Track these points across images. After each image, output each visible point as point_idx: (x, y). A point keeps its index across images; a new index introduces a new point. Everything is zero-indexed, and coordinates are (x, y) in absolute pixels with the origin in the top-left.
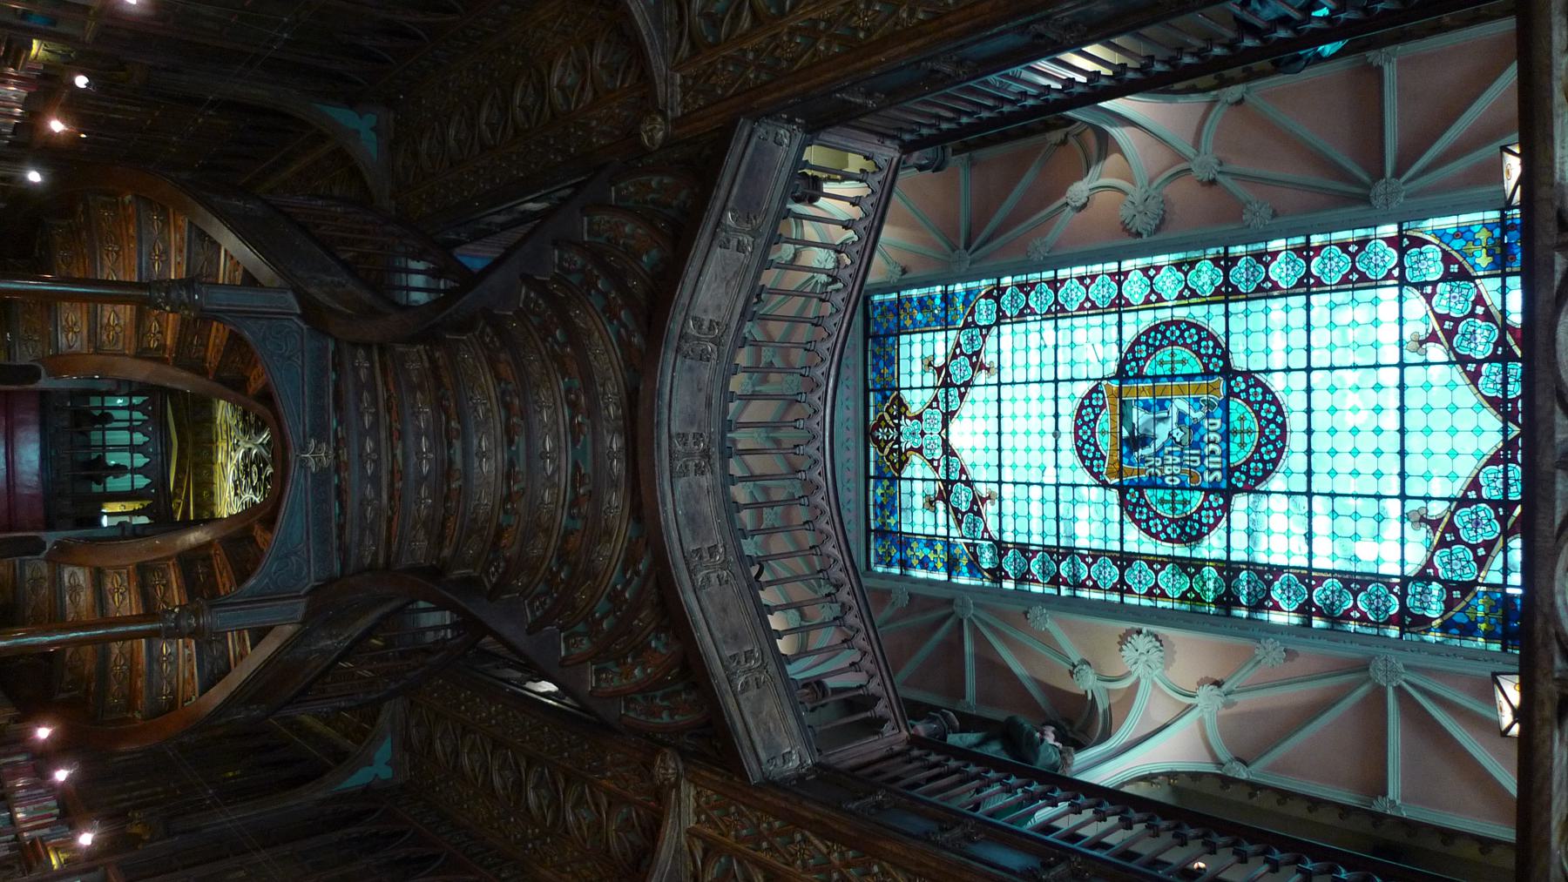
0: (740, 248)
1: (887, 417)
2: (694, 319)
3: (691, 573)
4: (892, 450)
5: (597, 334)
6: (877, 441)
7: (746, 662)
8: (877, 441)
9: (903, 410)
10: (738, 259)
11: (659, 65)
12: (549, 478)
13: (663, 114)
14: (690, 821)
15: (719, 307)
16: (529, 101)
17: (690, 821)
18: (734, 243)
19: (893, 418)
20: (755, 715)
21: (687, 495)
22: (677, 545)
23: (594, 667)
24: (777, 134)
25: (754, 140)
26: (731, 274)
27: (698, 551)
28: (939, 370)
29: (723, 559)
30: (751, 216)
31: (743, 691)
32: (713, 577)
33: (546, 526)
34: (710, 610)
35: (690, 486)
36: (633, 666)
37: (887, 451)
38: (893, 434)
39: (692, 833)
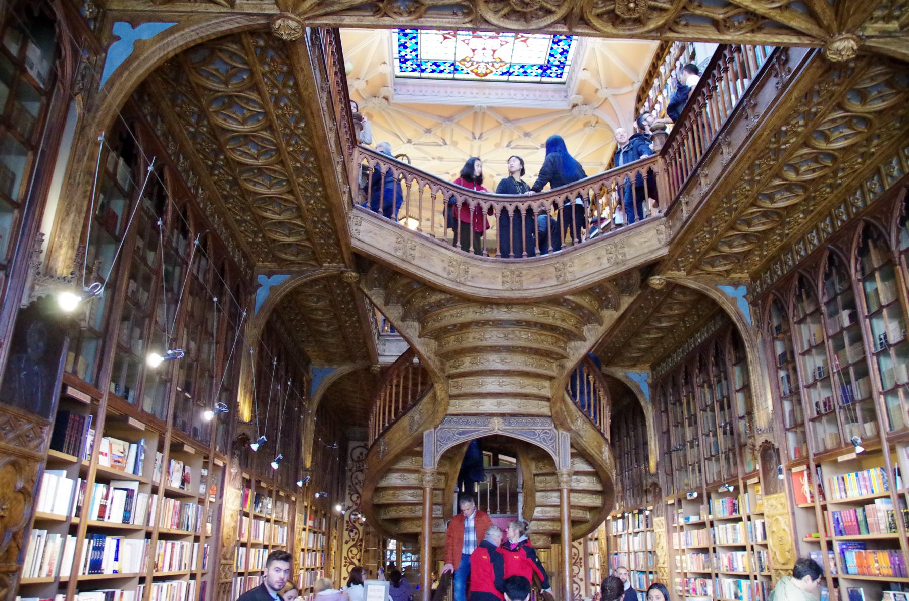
1: (472, 68)
4: (493, 66)
6: (486, 74)
8: (486, 74)
9: (468, 59)
11: (320, 273)
13: (342, 272)
14: (683, 273)
16: (320, 313)
17: (683, 273)
18: (412, 252)
19: (472, 65)
28: (445, 38)
36: (607, 298)
37: (492, 69)
38: (482, 65)
39: (689, 273)
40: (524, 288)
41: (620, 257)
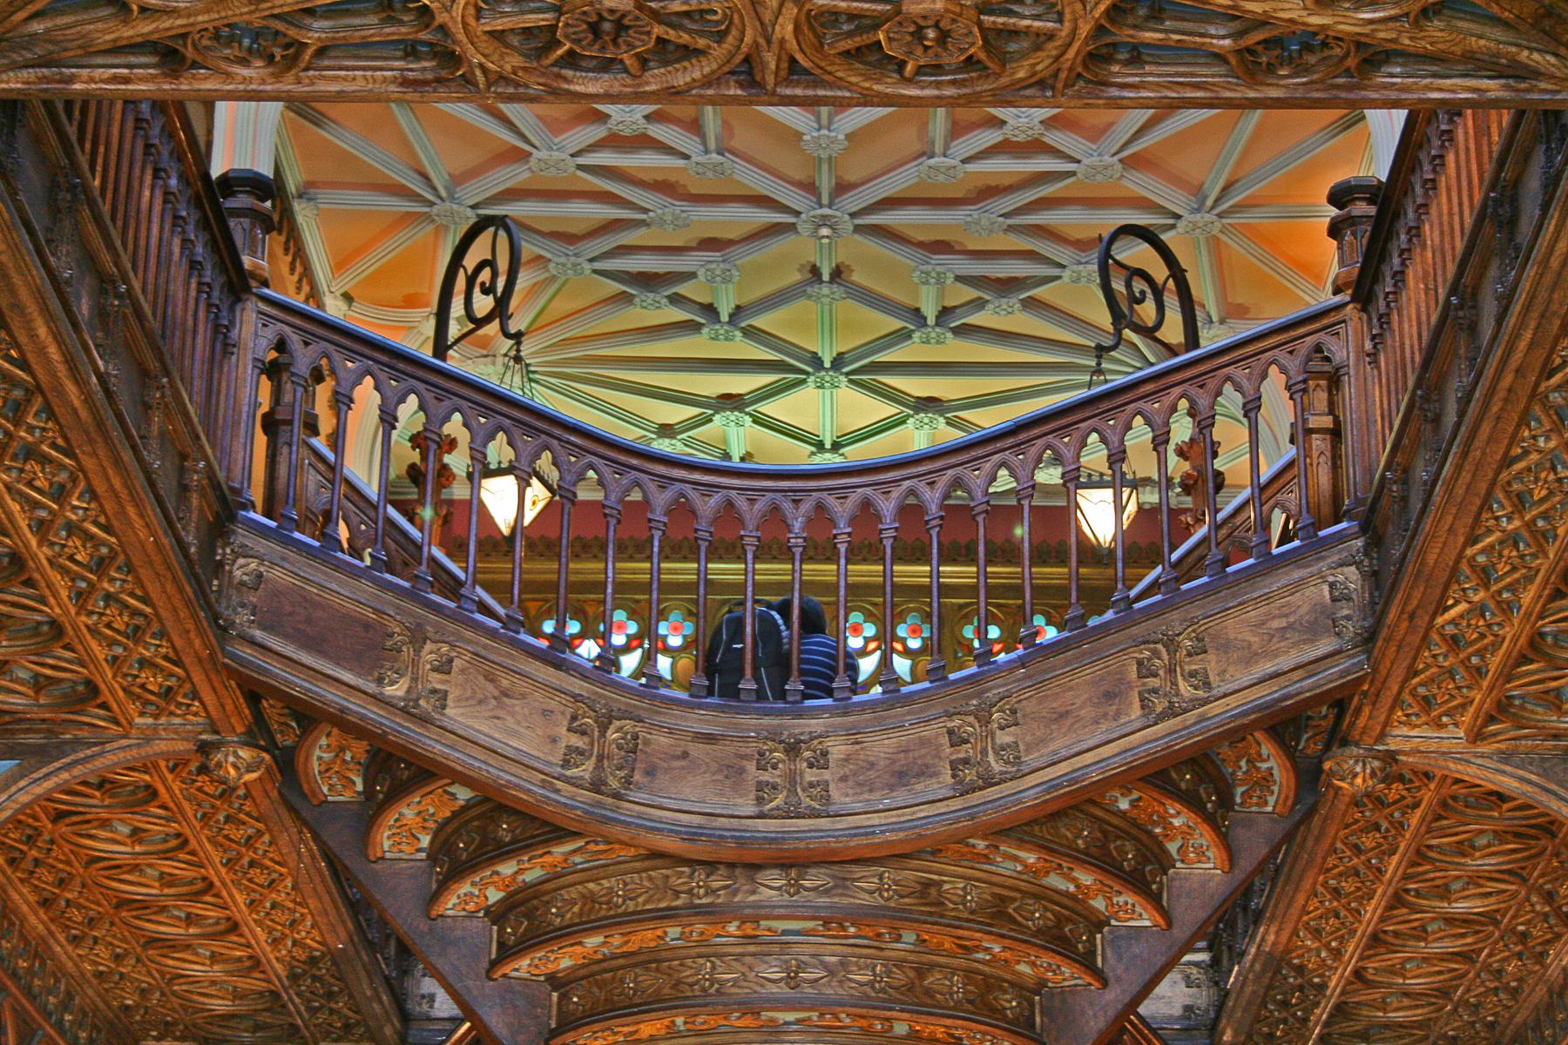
0: (444, 667)
2: (566, 764)
3: (988, 782)
5: (591, 885)
7: (1155, 675)
10: (462, 671)
12: (831, 972)
14: (1454, 736)
15: (547, 713)
18: (436, 682)
20: (1251, 658)
21: (860, 784)
22: (941, 808)
23: (1178, 865)
24: (242, 584)
25: (258, 634)
26: (490, 687)
27: (954, 766)
29: (971, 719)
30: (389, 643)
31: (1207, 685)
32: (1003, 738)
33: (912, 974)
34: (1060, 744)
35: (844, 779)
39: (1477, 736)
40: (833, 809)
41: (1185, 689)
